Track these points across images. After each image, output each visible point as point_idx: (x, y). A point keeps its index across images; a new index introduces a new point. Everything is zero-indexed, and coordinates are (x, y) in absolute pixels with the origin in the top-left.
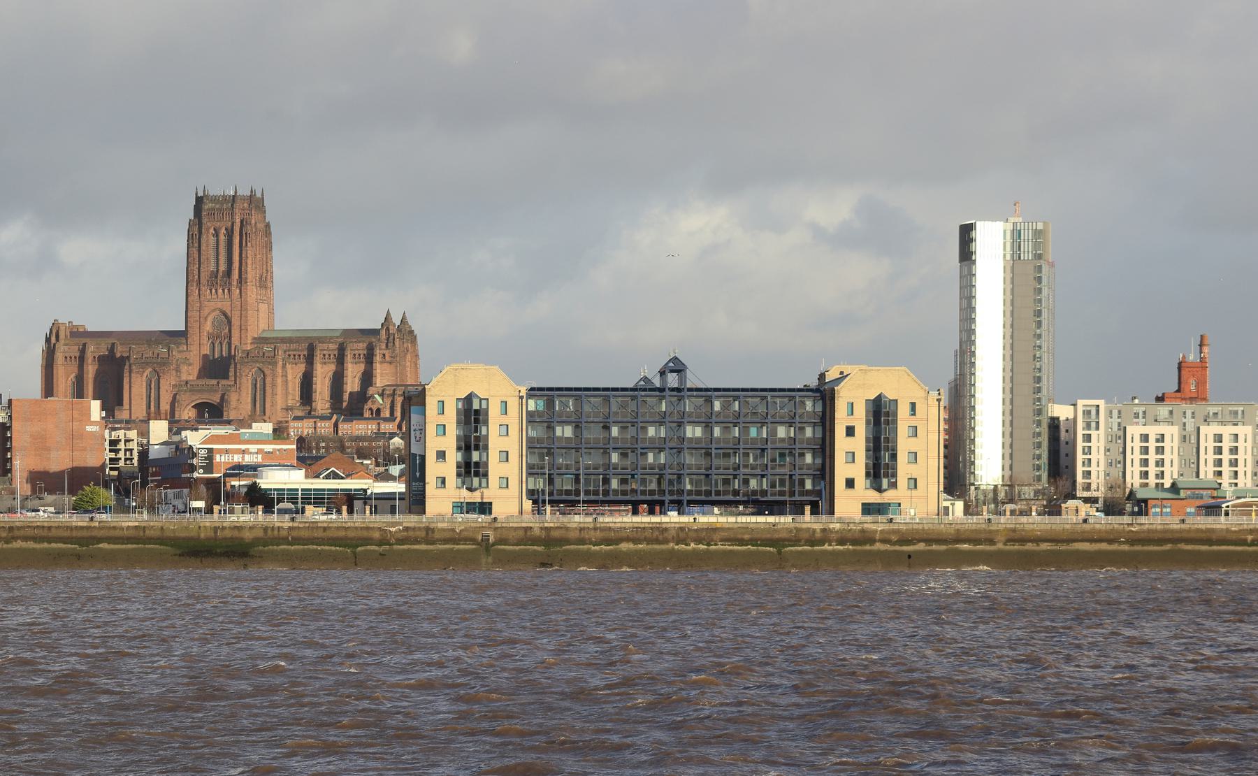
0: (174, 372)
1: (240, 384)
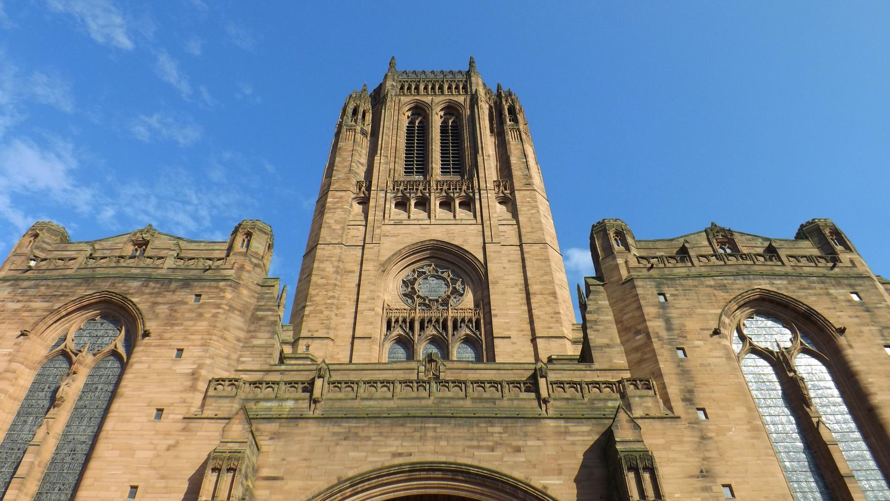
0: (237, 320)
1: (684, 373)
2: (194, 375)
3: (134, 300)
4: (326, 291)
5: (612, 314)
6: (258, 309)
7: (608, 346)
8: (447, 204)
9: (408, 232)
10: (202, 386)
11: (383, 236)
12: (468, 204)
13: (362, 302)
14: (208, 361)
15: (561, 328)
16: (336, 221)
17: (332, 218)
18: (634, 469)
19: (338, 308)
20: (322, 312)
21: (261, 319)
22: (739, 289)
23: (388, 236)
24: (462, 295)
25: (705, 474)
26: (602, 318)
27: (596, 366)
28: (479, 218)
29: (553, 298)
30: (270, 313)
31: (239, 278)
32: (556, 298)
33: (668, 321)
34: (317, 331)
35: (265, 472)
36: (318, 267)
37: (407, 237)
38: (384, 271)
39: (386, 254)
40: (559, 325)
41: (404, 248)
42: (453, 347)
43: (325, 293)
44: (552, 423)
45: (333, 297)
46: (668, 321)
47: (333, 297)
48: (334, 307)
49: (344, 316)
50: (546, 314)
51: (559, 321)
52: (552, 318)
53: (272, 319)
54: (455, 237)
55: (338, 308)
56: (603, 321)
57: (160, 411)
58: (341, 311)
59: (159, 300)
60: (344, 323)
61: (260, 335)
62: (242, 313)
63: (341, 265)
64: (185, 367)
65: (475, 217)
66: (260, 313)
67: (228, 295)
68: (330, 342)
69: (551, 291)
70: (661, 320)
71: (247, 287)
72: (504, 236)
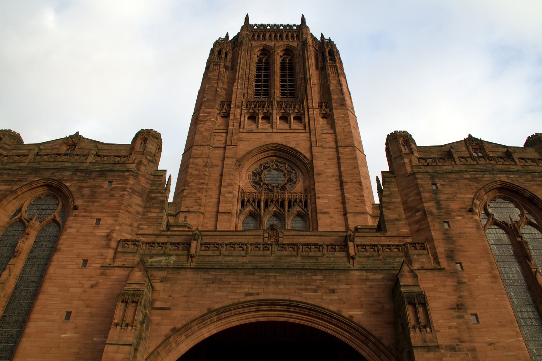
0: (137, 200)
1: (448, 238)
2: (108, 237)
3: (68, 184)
4: (199, 179)
5: (400, 197)
6: (152, 191)
7: (397, 220)
8: (284, 118)
9: (257, 138)
10: (114, 244)
11: (239, 140)
12: (298, 118)
13: (224, 187)
14: (117, 228)
15: (364, 207)
16: (206, 129)
17: (203, 128)
18: (413, 304)
19: (206, 191)
20: (195, 194)
21: (154, 198)
22: (486, 181)
23: (242, 140)
24: (295, 183)
25: (459, 307)
26: (393, 200)
27: (388, 234)
28: (307, 128)
29: (359, 186)
30: (160, 195)
31: (139, 170)
32: (361, 185)
33: (438, 203)
34: (192, 207)
35: (158, 304)
36: (193, 162)
37: (256, 141)
38: (239, 165)
39: (241, 153)
40: (362, 205)
41: (254, 149)
42: (288, 220)
43: (198, 180)
44: (357, 273)
45: (203, 183)
46: (438, 203)
47: (203, 183)
48: (204, 190)
49: (211, 197)
50: (354, 197)
51: (363, 202)
52: (358, 199)
53: (161, 199)
54: (290, 141)
55: (206, 191)
56: (394, 202)
57: (85, 261)
58: (208, 193)
59: (84, 185)
60: (211, 202)
61: (153, 210)
62: (140, 195)
63: (209, 160)
64: (102, 232)
65: (305, 127)
66: (153, 195)
67: (131, 182)
68: (202, 216)
69: (358, 181)
70: (434, 202)
71: (144, 176)
72: (325, 141)
